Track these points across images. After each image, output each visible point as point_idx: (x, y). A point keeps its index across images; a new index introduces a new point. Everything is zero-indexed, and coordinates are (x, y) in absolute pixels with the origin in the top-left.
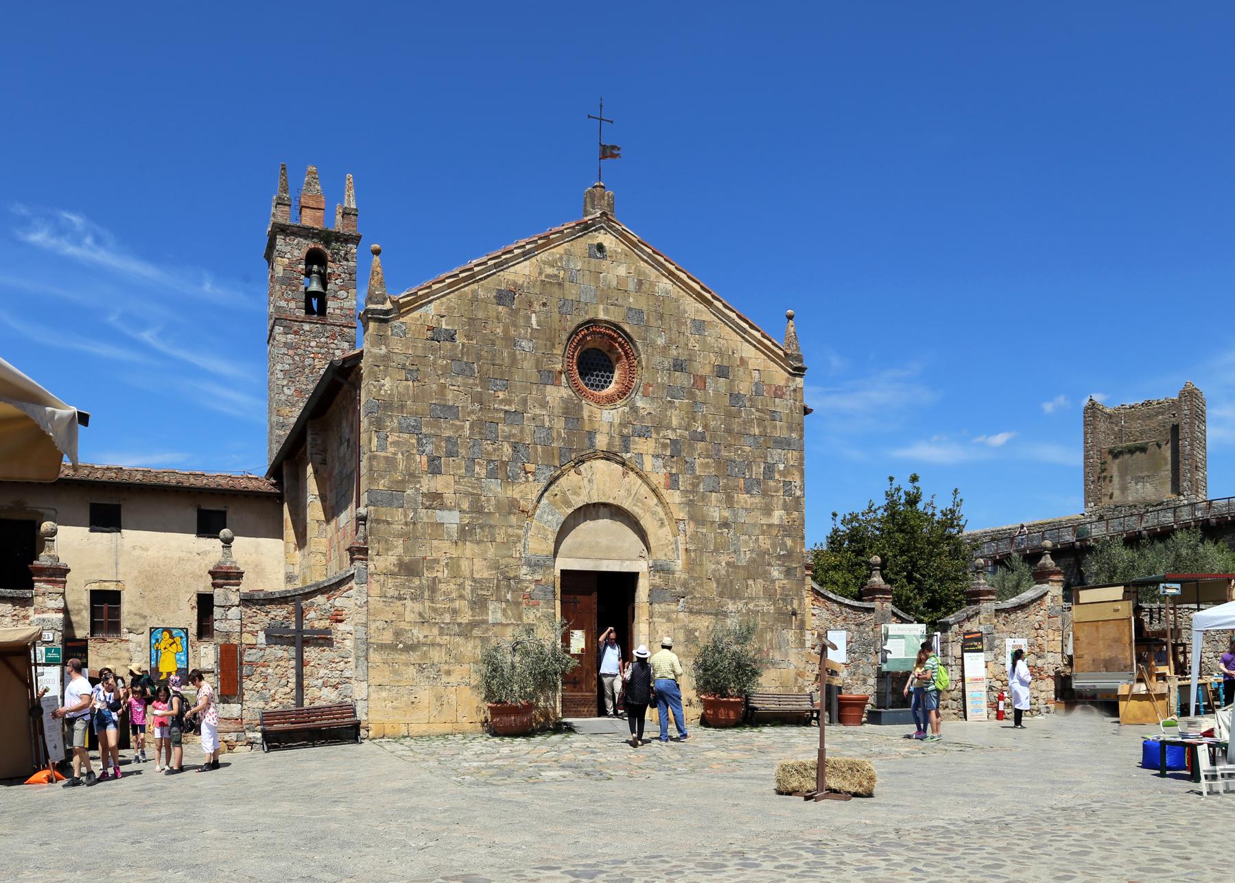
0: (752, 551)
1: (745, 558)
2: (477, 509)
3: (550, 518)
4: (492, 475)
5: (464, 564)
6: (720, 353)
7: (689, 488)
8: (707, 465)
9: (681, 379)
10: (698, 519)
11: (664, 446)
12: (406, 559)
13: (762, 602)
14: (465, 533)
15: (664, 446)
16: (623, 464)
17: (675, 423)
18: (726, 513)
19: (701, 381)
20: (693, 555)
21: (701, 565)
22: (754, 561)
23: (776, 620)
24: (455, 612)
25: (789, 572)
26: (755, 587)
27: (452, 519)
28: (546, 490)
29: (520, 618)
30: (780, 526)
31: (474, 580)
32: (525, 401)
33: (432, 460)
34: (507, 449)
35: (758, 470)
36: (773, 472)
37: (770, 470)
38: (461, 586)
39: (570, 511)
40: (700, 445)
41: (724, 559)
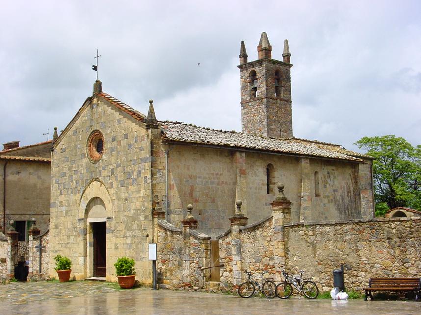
0: (134, 209)
1: (131, 213)
2: (69, 206)
3: (84, 205)
4: (71, 193)
5: (66, 223)
6: (125, 130)
7: (116, 187)
8: (121, 176)
9: (115, 143)
10: (119, 199)
11: (109, 172)
12: (56, 223)
13: (137, 231)
14: (67, 212)
15: (109, 172)
16: (100, 181)
17: (112, 162)
18: (126, 195)
19: (119, 142)
20: (117, 213)
21: (119, 217)
22: (135, 213)
23: (142, 239)
24: (64, 239)
25: (146, 217)
26: (135, 225)
27: (64, 209)
28: (82, 195)
29: (76, 241)
30: (143, 197)
31: (68, 229)
32: (78, 166)
33: (61, 190)
34: (75, 183)
35: (136, 174)
36: (140, 174)
37: (140, 173)
38: (65, 231)
39: (88, 202)
40: (119, 169)
41: (126, 214)
